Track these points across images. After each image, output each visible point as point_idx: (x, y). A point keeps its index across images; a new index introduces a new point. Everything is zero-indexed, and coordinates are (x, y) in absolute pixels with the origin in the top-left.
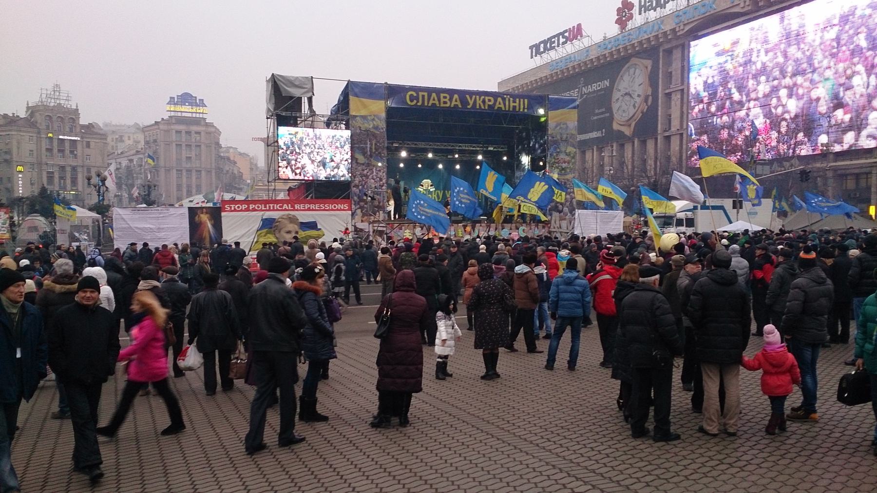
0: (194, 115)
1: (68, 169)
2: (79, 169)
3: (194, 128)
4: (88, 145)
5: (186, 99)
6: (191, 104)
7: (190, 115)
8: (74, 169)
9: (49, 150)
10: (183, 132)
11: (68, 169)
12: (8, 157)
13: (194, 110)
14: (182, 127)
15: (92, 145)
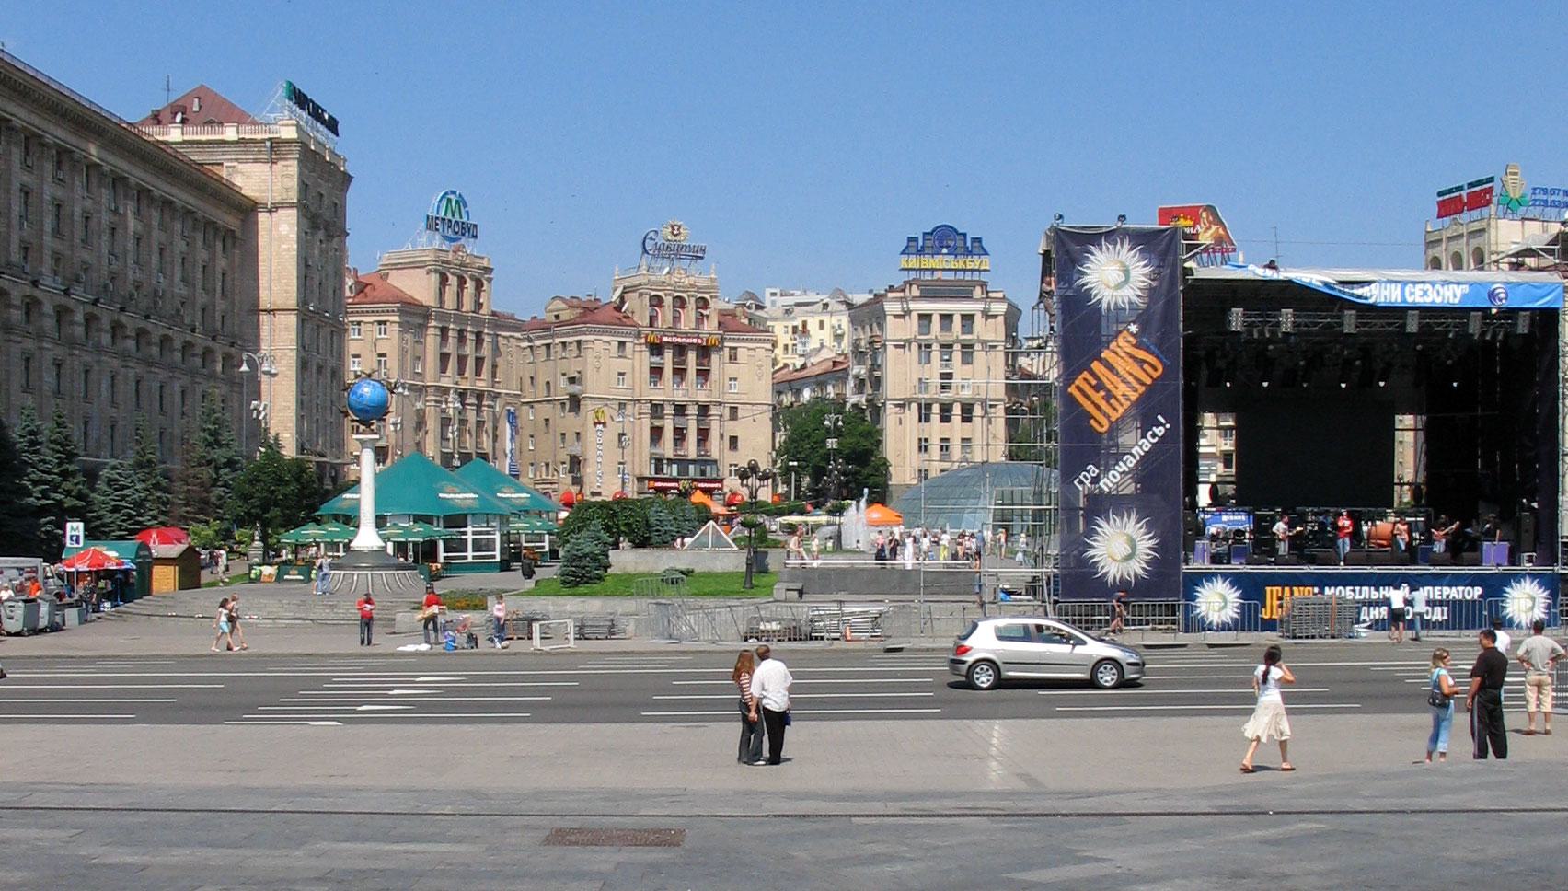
0: (960, 275)
1: (692, 410)
2: (714, 411)
3: (957, 307)
4: (733, 357)
5: (944, 238)
6: (954, 252)
7: (950, 276)
8: (704, 410)
9: (656, 372)
10: (936, 319)
11: (692, 410)
12: (575, 389)
13: (961, 265)
14: (936, 307)
15: (742, 354)
